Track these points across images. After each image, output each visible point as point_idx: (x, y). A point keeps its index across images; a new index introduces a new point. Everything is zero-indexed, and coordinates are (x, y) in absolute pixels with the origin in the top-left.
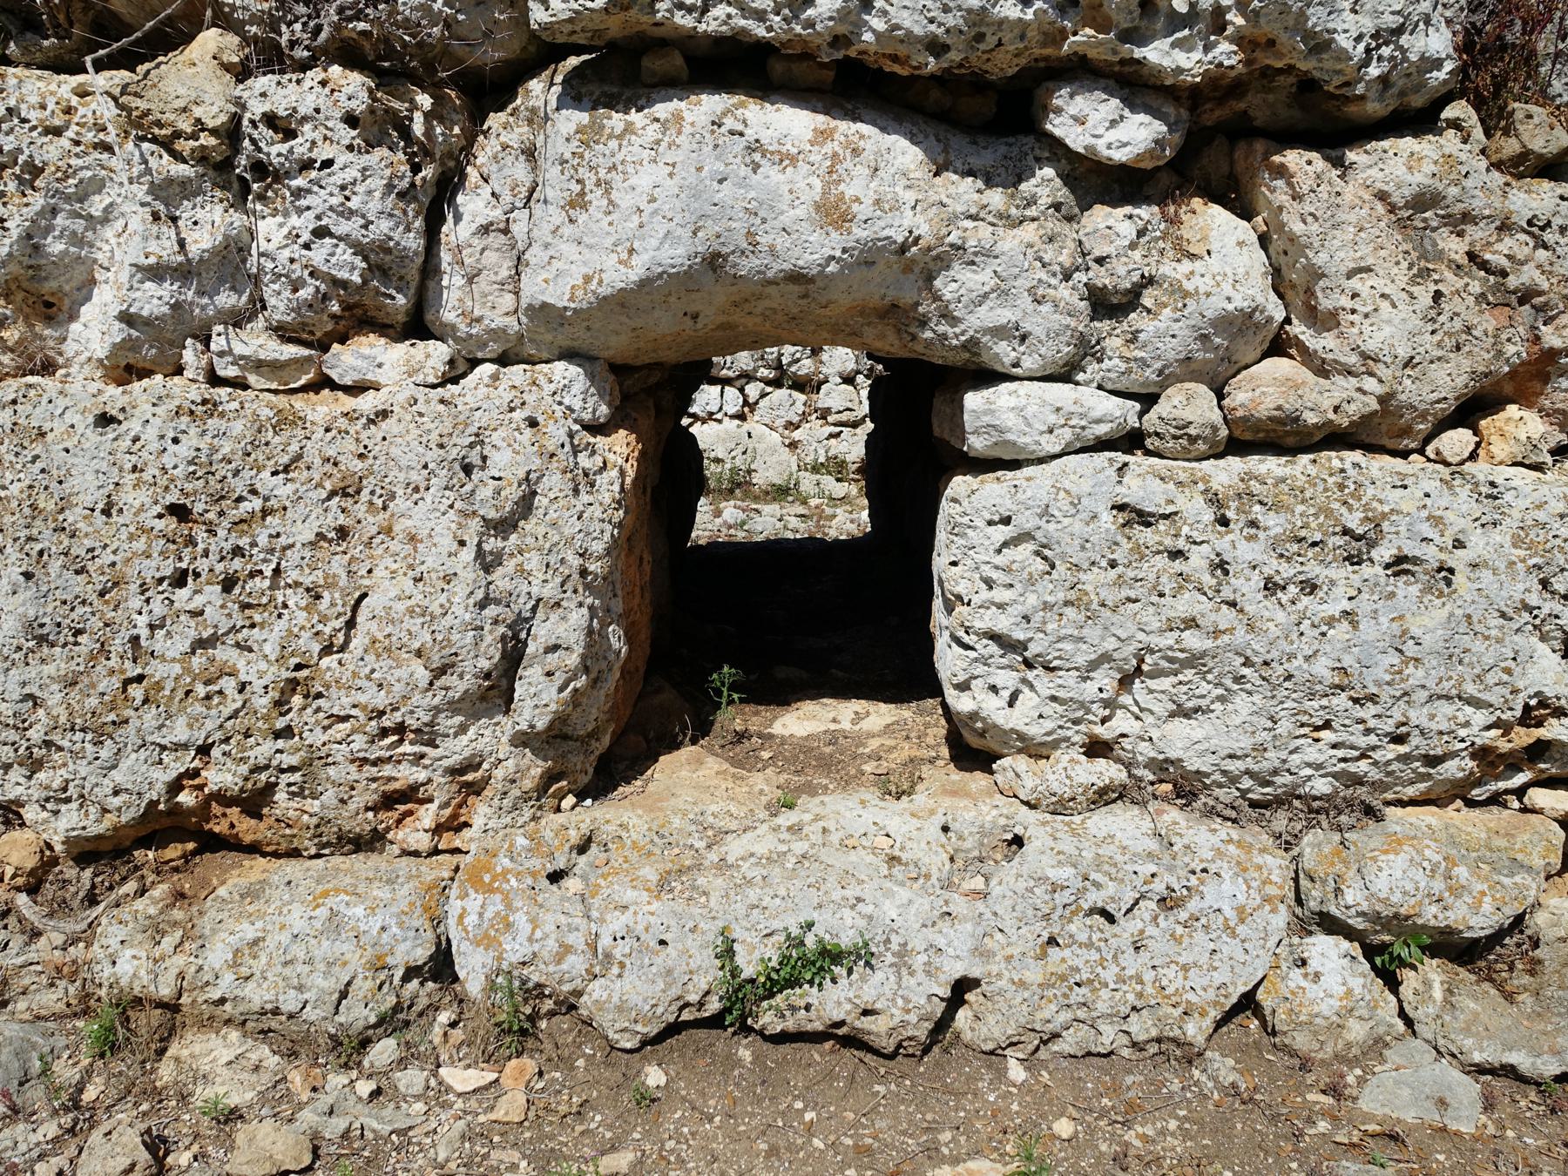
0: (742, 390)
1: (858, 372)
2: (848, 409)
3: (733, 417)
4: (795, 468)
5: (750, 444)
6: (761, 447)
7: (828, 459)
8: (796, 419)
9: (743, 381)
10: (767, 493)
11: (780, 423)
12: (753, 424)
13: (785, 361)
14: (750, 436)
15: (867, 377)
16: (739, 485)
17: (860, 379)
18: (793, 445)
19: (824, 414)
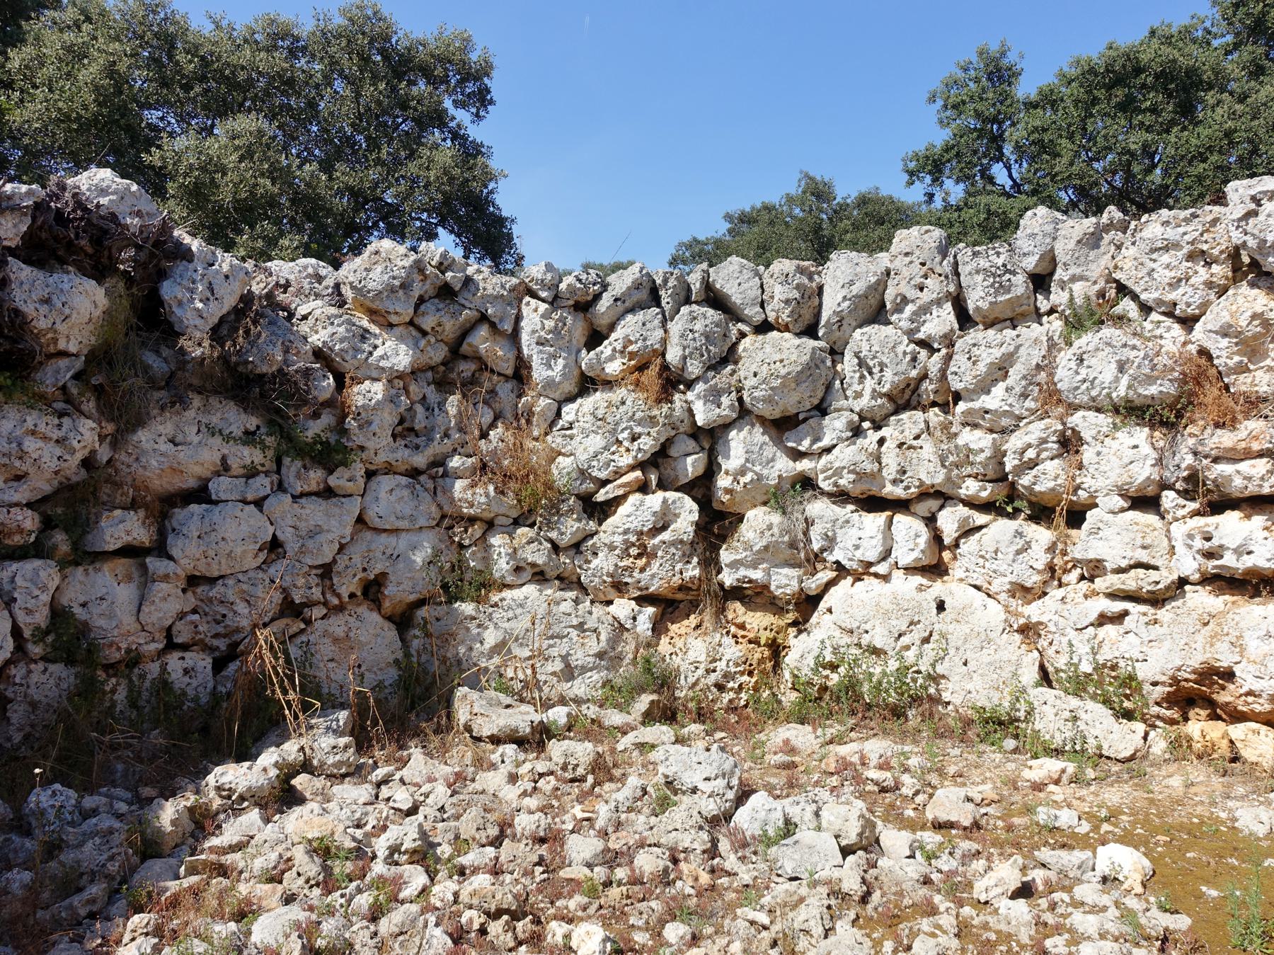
0: (930, 520)
1: (1164, 486)
2: (1147, 567)
3: (910, 570)
4: (1030, 674)
5: (942, 624)
6: (957, 632)
7: (1098, 668)
8: (1032, 580)
9: (933, 504)
10: (968, 723)
11: (1000, 585)
12: (951, 588)
13: (1010, 463)
14: (941, 607)
15: (1187, 494)
16: (916, 700)
17: (1169, 499)
18: (1029, 631)
19: (1094, 569)
